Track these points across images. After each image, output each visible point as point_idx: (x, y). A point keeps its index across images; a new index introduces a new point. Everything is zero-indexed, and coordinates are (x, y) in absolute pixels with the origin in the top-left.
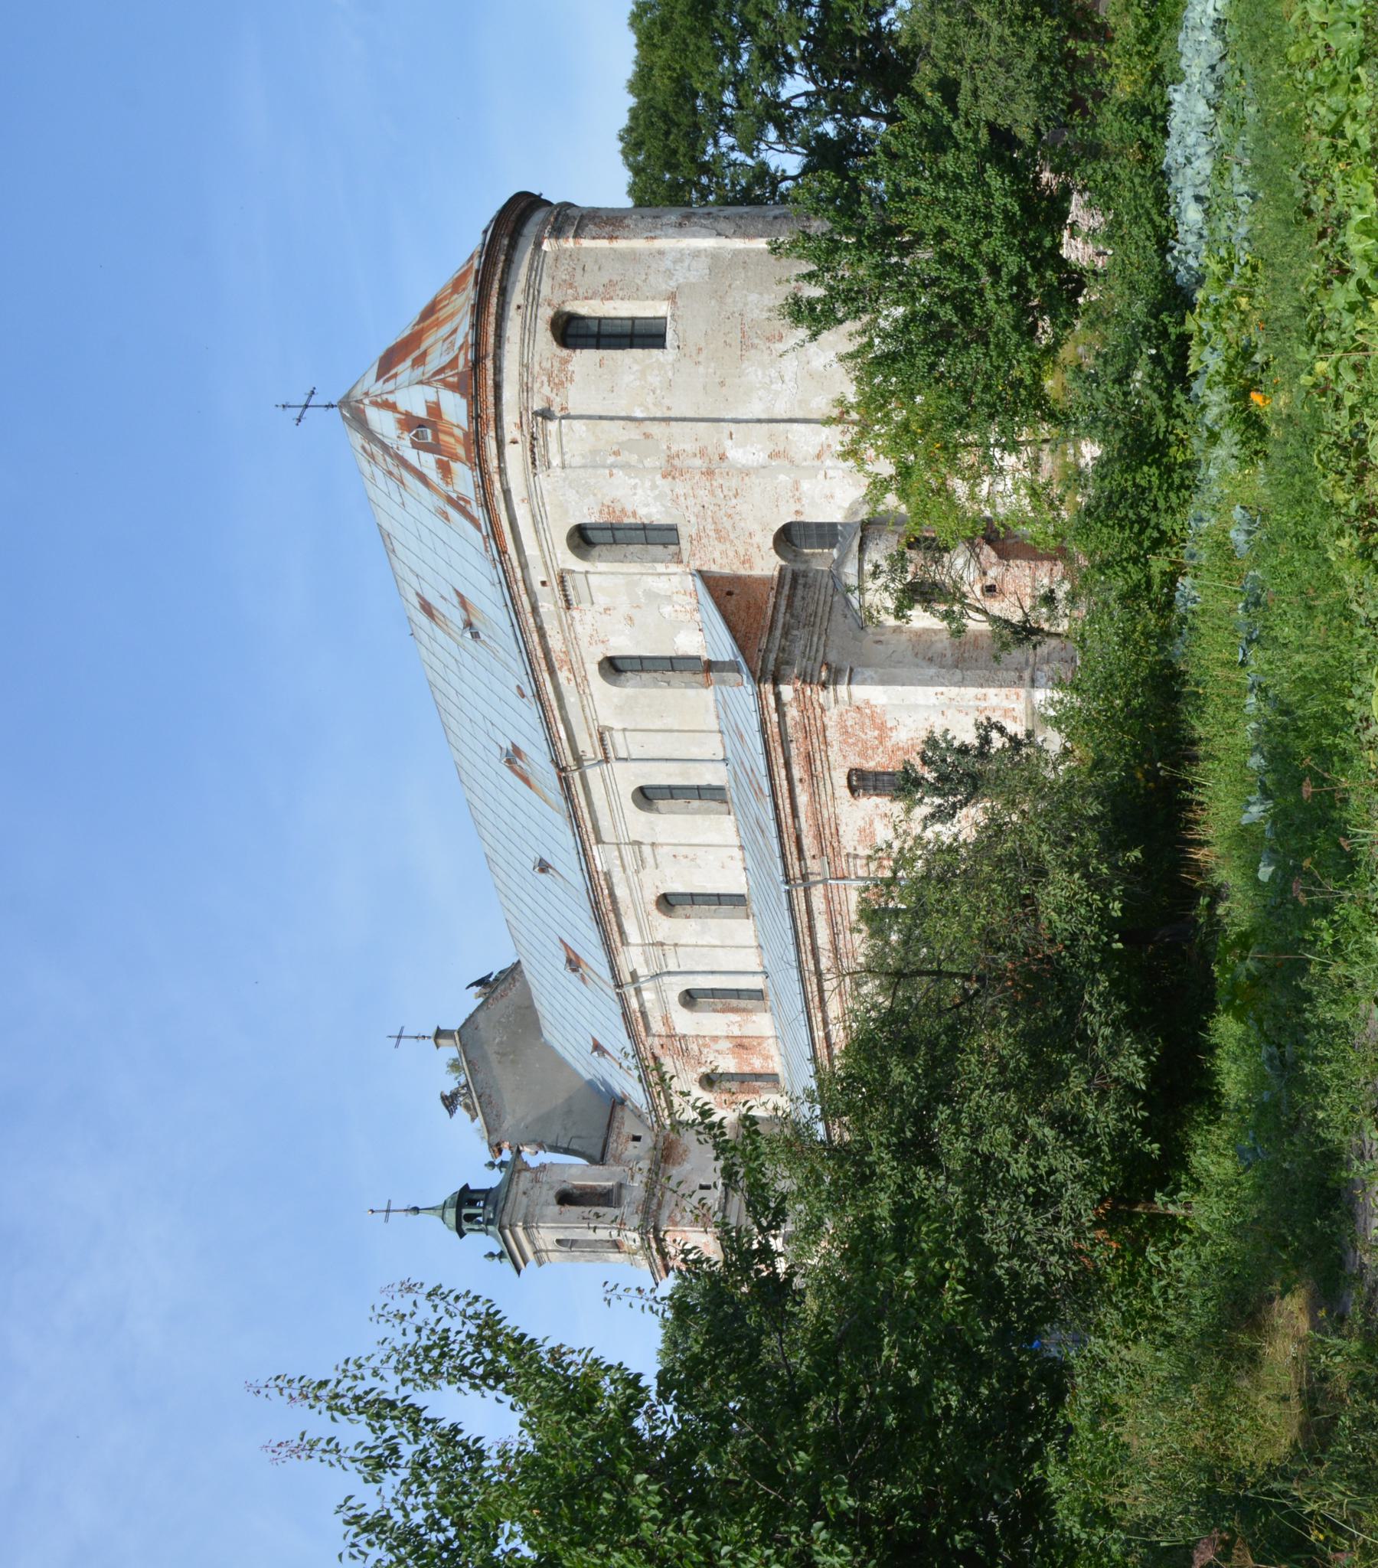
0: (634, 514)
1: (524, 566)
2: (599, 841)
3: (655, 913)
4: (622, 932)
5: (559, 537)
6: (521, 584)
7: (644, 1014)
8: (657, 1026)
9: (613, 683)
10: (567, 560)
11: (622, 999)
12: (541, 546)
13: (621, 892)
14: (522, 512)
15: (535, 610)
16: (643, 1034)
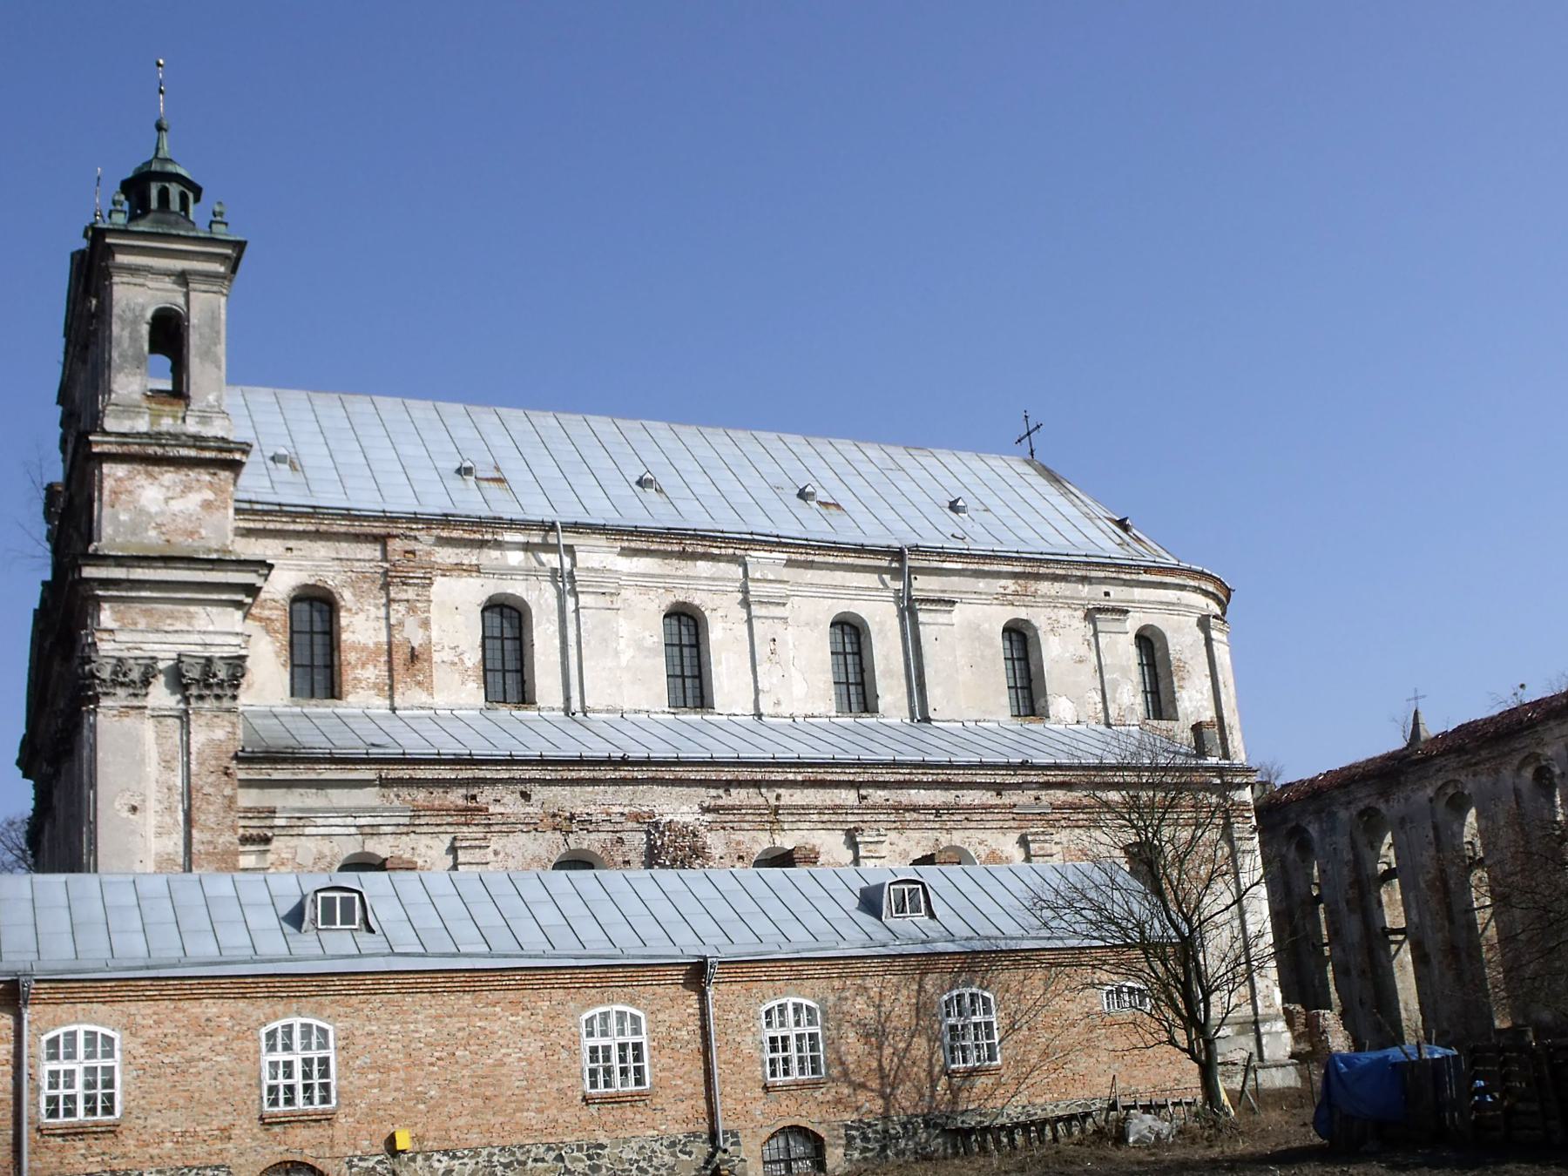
0: (1181, 687)
1: (1126, 583)
2: (790, 563)
3: (668, 600)
4: (636, 552)
5: (1157, 620)
6: (1114, 575)
7: (482, 544)
8: (446, 555)
9: (1035, 630)
10: (1133, 623)
11: (525, 526)
12: (1150, 603)
13: (703, 567)
14: (1171, 595)
15: (1084, 580)
16: (445, 534)
